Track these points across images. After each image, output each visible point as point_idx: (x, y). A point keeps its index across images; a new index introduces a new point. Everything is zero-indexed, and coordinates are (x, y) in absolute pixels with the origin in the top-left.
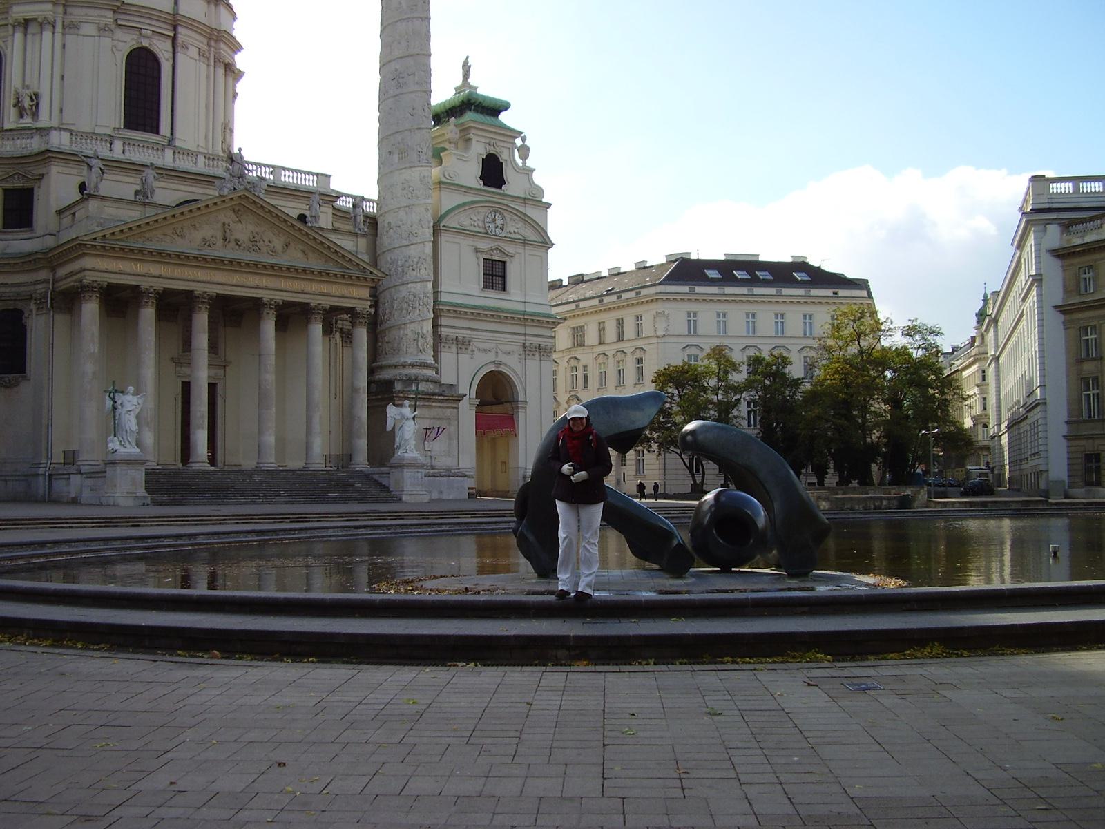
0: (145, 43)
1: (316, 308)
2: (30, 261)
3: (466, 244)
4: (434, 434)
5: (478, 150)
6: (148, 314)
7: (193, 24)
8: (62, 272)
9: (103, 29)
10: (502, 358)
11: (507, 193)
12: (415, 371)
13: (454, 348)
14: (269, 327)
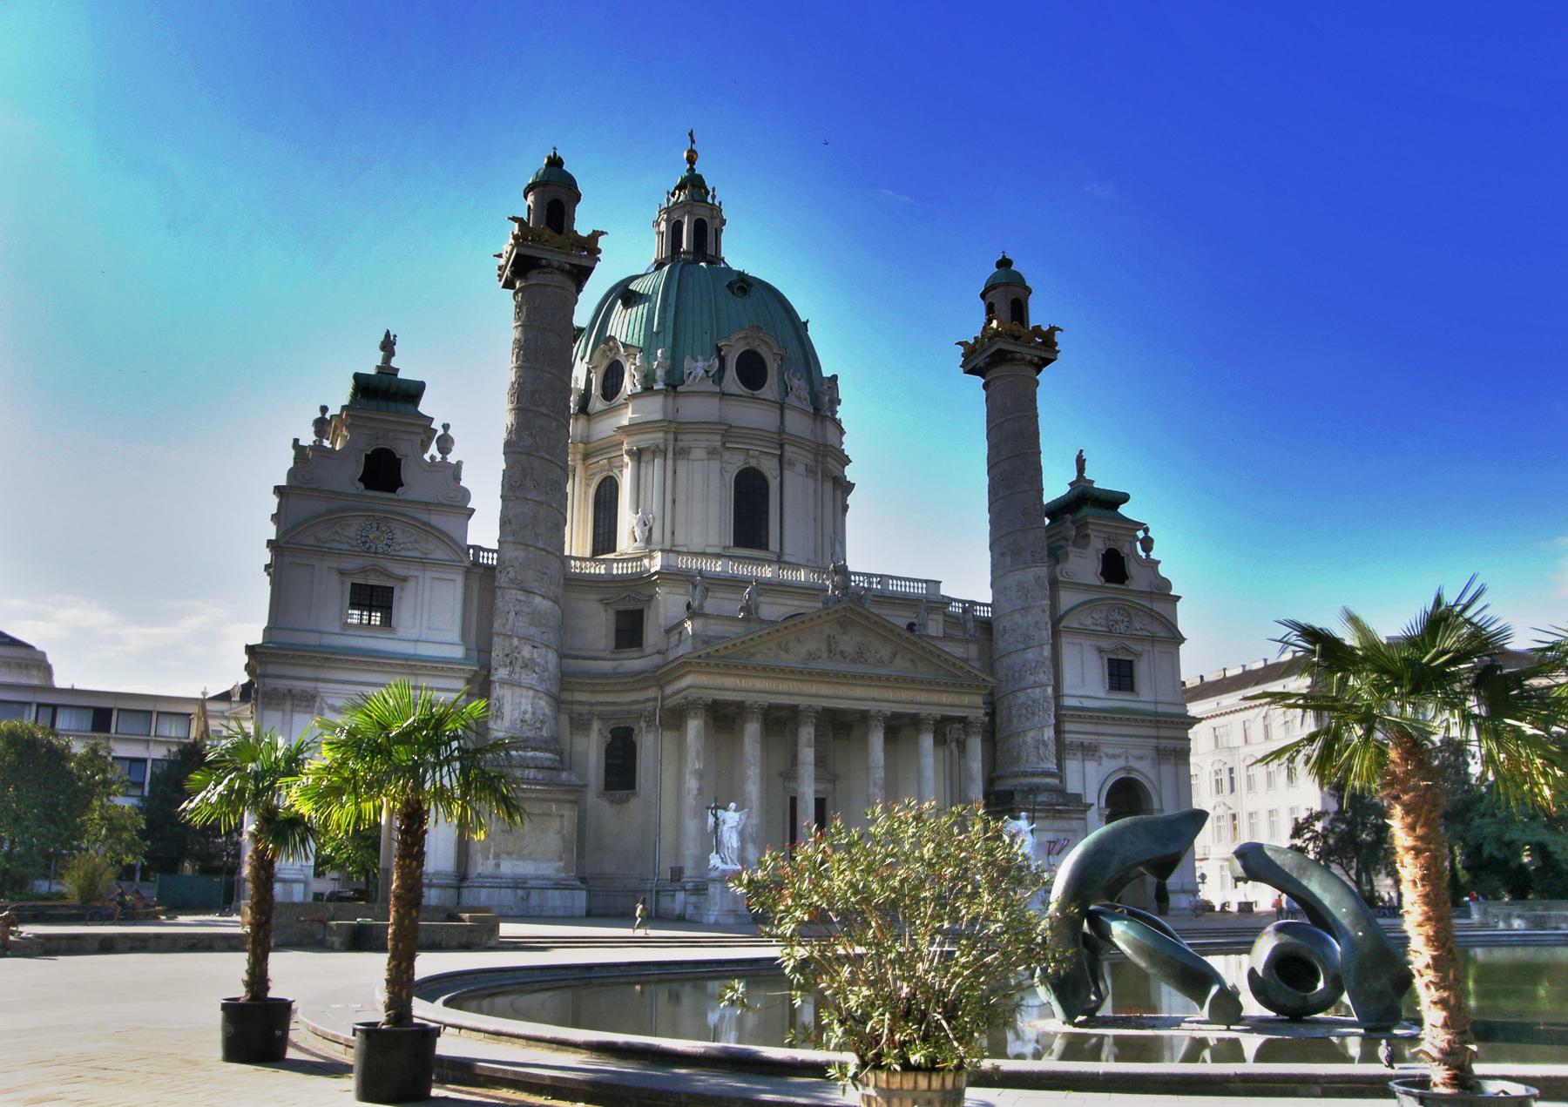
0: (753, 463)
2: (640, 679)
3: (1088, 643)
4: (1058, 847)
5: (1097, 545)
6: (752, 729)
7: (798, 442)
8: (669, 690)
9: (712, 453)
12: (1037, 780)
13: (1079, 755)
14: (877, 740)
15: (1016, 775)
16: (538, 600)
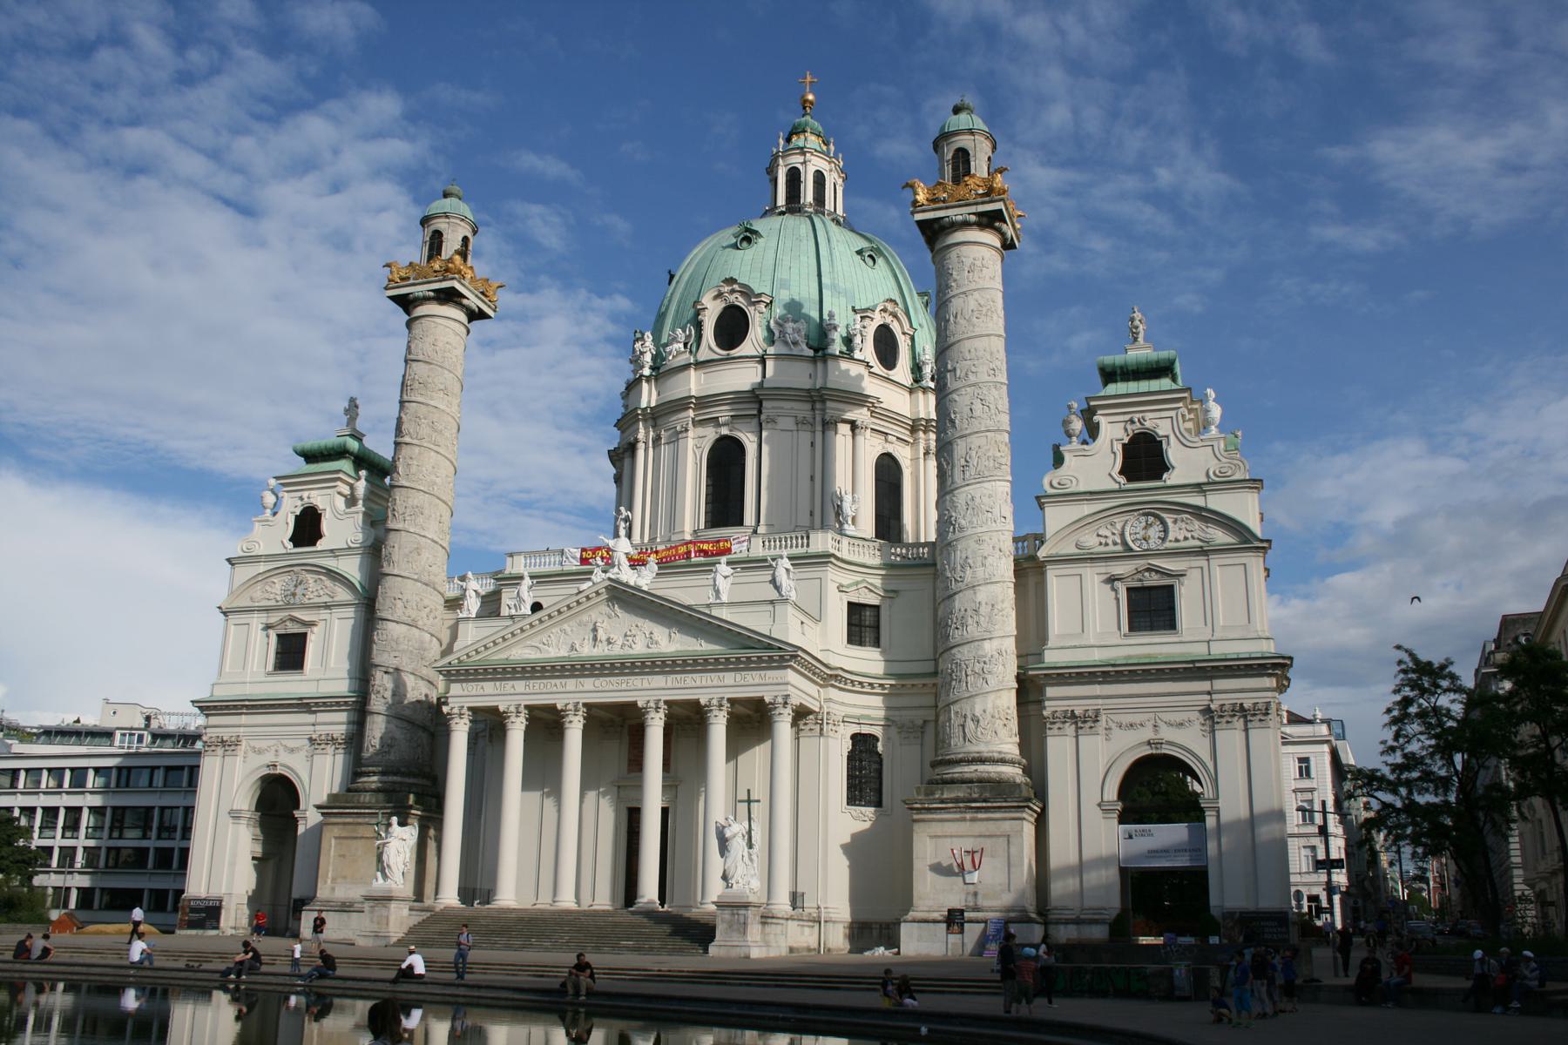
0: (725, 431)
3: (1093, 576)
5: (1113, 432)
10: (1167, 734)
11: (1169, 483)
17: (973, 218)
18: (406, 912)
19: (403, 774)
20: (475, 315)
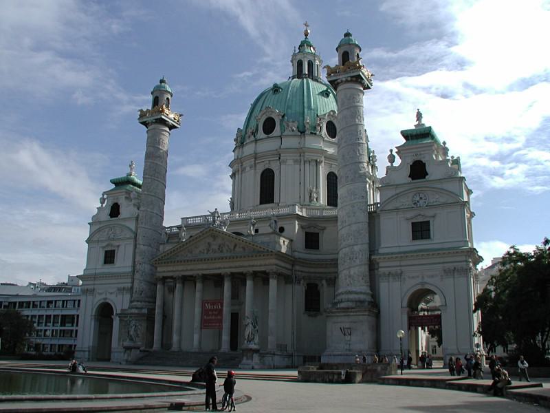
0: (267, 167)
1: (246, 274)
10: (426, 280)
11: (430, 179)
13: (391, 279)
14: (227, 285)
15: (340, 294)
16: (142, 246)
17: (349, 79)
18: (138, 352)
19: (145, 302)
20: (172, 127)
